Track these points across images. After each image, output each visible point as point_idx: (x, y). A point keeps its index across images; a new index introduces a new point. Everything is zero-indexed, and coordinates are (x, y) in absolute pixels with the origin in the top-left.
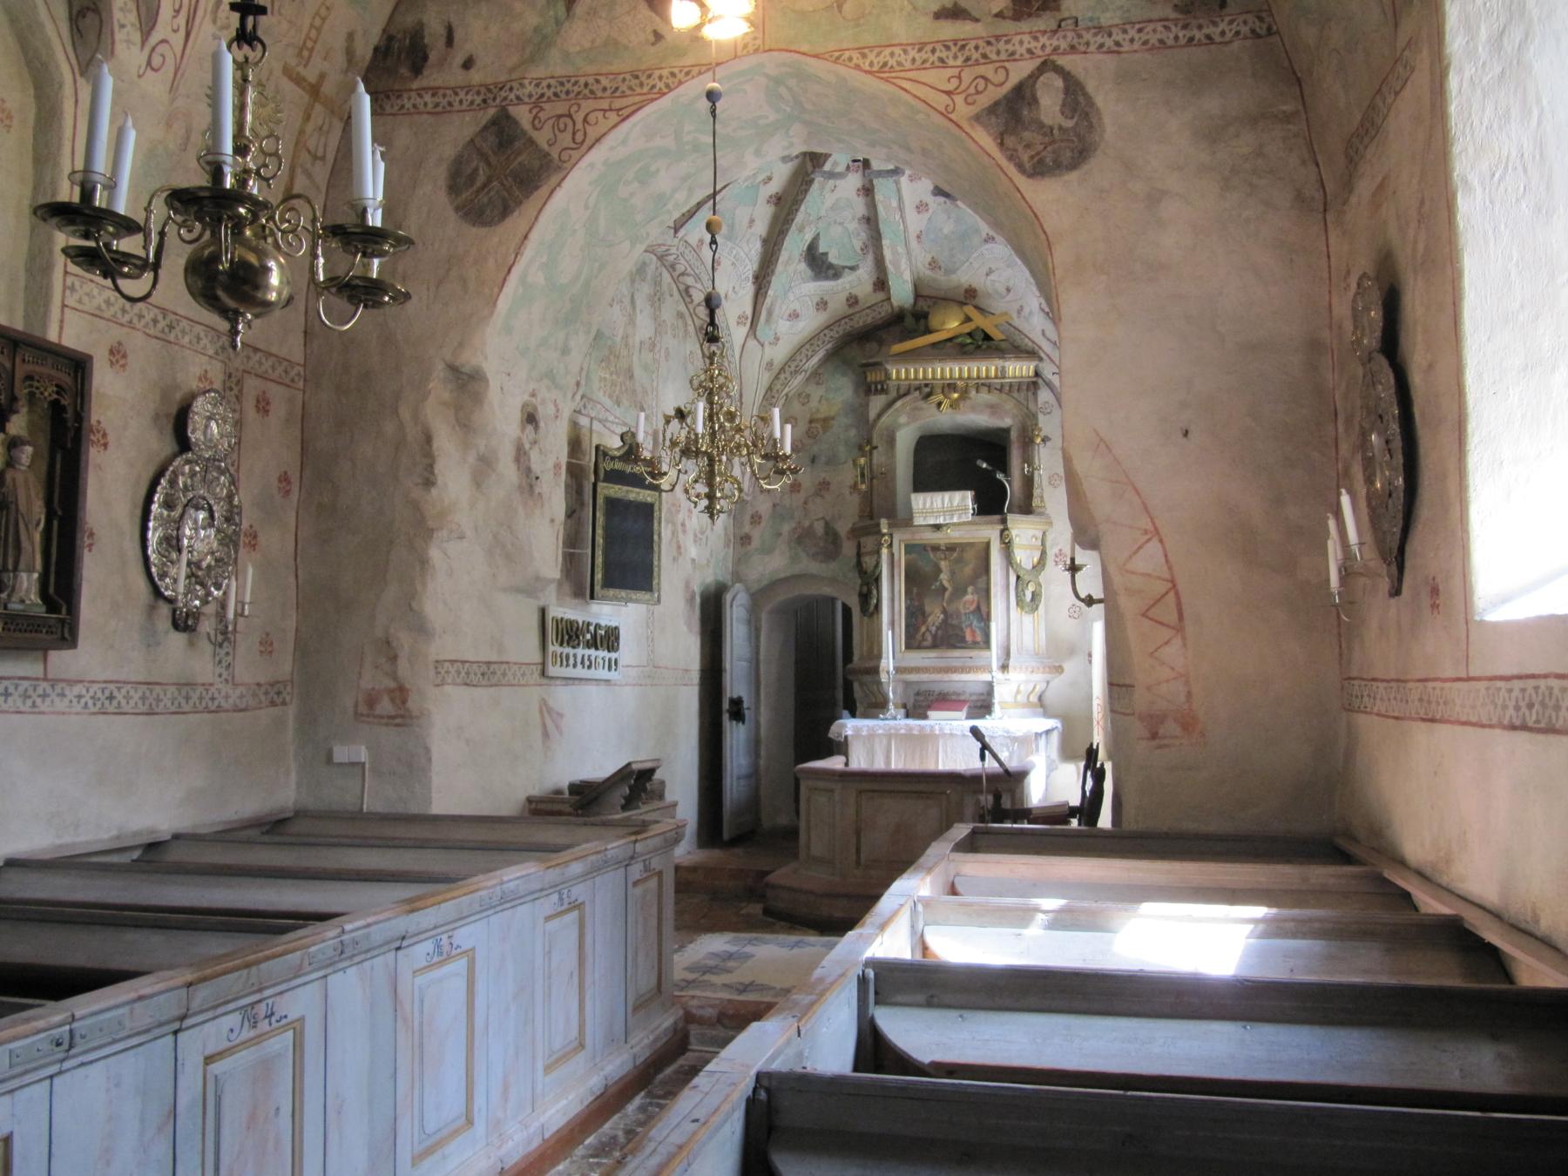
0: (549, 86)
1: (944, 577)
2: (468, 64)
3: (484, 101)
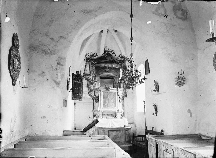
1: (109, 97)
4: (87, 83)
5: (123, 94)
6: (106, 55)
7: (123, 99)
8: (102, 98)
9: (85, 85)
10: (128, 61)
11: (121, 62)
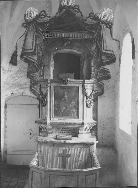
1: (66, 96)
4: (28, 68)
5: (95, 89)
6: (63, 14)
7: (96, 100)
8: (53, 98)
9: (25, 72)
10: (105, 26)
11: (92, 27)
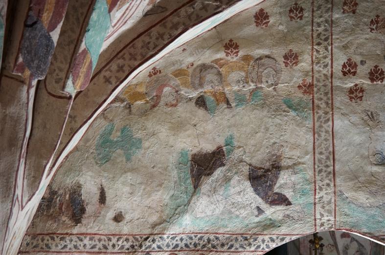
0: (182, 240)
2: (118, 218)
3: (132, 247)
